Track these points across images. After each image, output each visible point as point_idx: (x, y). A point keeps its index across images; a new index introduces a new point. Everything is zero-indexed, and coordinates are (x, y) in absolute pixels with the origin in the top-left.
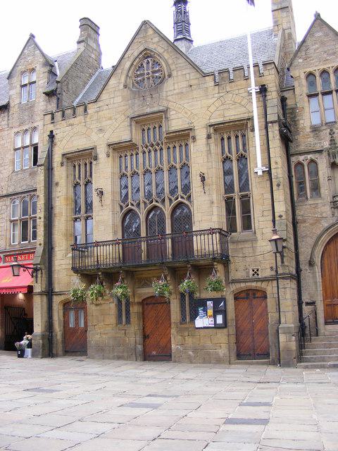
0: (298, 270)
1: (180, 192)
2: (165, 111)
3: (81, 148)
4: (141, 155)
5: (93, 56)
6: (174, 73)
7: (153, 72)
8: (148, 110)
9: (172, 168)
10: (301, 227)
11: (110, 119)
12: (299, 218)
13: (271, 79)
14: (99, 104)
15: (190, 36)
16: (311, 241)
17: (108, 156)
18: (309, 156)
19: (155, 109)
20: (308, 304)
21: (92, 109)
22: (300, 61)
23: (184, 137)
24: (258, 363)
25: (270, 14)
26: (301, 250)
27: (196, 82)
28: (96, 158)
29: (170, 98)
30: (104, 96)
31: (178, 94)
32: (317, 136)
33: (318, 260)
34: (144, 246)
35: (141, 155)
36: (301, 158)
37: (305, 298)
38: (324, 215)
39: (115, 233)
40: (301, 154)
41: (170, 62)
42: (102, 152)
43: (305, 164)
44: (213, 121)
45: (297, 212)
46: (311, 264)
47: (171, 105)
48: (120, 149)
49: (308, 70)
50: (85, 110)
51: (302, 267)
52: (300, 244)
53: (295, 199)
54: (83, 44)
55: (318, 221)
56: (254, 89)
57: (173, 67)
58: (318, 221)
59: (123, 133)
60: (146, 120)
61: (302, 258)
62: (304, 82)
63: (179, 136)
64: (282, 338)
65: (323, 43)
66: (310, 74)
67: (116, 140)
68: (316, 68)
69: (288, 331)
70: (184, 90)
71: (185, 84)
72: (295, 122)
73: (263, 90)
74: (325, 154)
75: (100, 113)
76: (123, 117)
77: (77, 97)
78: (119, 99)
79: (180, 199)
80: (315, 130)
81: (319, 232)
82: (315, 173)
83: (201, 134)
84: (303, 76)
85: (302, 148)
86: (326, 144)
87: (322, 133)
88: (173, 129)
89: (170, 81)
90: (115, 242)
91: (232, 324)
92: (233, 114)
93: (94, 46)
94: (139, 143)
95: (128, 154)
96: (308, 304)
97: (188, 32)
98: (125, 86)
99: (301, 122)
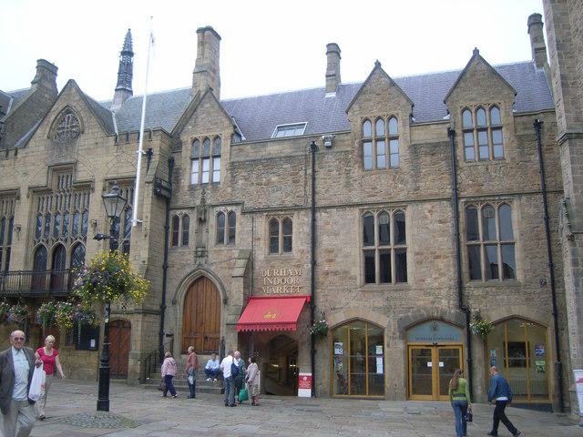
0: (163, 307)
1: (79, 235)
2: (76, 164)
3: (9, 187)
4: (54, 198)
5: (46, 96)
6: (86, 131)
7: (72, 127)
8: (63, 161)
9: (76, 212)
10: (170, 271)
11: (34, 165)
12: (170, 263)
13: (156, 144)
14: (27, 150)
15: (130, 86)
16: (176, 283)
17: (28, 197)
18: (184, 211)
19: (68, 161)
20: (168, 336)
21: (21, 153)
22: (190, 127)
23: (87, 187)
24: (117, 382)
25: (191, 76)
26: (168, 290)
27: (101, 140)
28: (19, 198)
29: (80, 152)
30: (32, 144)
31: (85, 149)
32: (192, 195)
33: (181, 300)
34: (48, 277)
35: (54, 198)
36: (178, 212)
37: (167, 331)
38: (189, 262)
39: (26, 263)
40: (178, 209)
41: (85, 119)
42: (24, 193)
43: (180, 217)
44: (109, 176)
45: (169, 258)
46: (174, 302)
47: (80, 159)
48: (37, 192)
49: (194, 136)
50: (16, 154)
51: (167, 304)
52: (167, 284)
53: (169, 246)
54: (36, 85)
55: (183, 266)
56: (140, 151)
57: (86, 125)
58: (183, 266)
59: (41, 179)
60: (62, 169)
61: (167, 296)
62: (190, 146)
63: (83, 186)
64: (131, 362)
65: (209, 114)
66: (196, 140)
67: (35, 184)
68: (200, 135)
69: (135, 357)
70: (91, 147)
71: (93, 141)
72: (178, 181)
73: (149, 154)
74: (196, 210)
75: (27, 159)
76: (43, 165)
77: (23, 136)
78: (42, 148)
79: (59, 241)
80: (192, 188)
81: (182, 277)
82: (186, 226)
83: (99, 186)
84: (190, 141)
85: (180, 204)
86: (198, 202)
87: (196, 193)
88: (79, 179)
89: (82, 137)
90: (25, 273)
91: (101, 347)
92: (124, 172)
93: (49, 86)
94: (54, 188)
95: (45, 196)
96: (168, 336)
97: (130, 83)
98: (48, 138)
99: (183, 181)
